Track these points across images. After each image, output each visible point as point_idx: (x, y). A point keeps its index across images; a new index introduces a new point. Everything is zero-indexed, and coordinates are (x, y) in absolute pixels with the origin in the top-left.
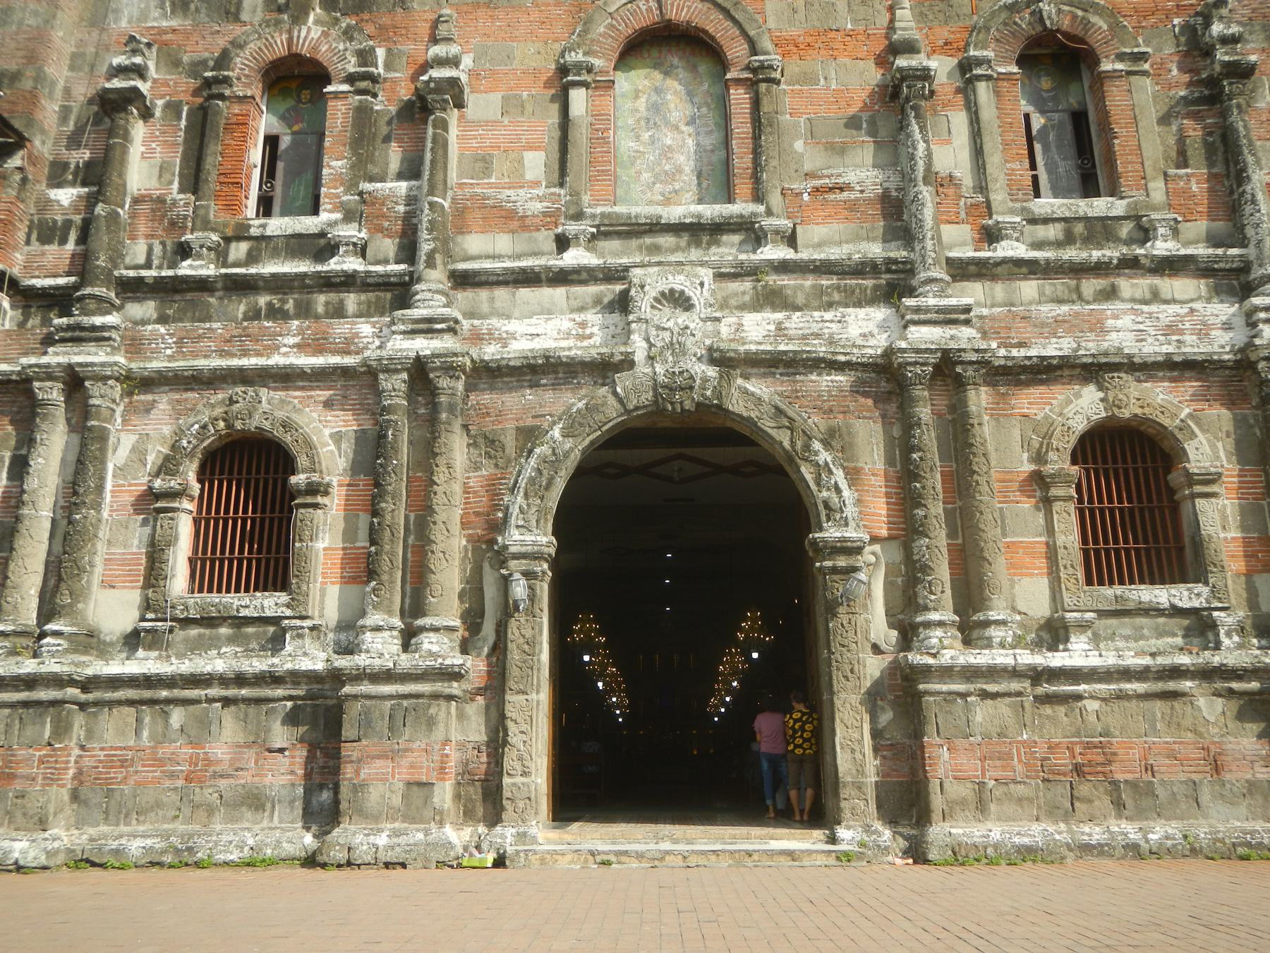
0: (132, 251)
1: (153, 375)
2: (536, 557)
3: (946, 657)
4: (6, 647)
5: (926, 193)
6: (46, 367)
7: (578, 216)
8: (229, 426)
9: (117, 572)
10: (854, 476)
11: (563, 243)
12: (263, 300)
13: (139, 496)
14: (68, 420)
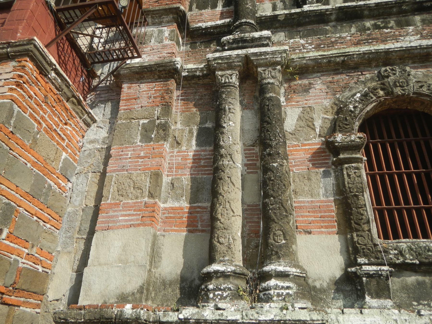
0: (261, 8)
1: (310, 62)
4: (229, 289)
6: (227, 59)
8: (387, 94)
9: (310, 219)
12: (368, 24)
13: (314, 153)
14: (241, 103)
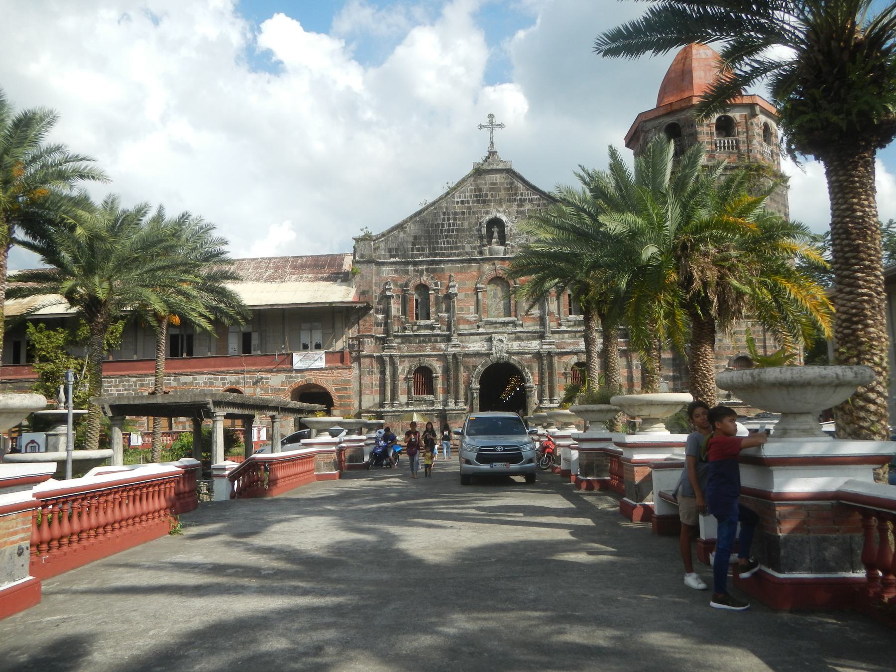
2: (477, 389)
3: (546, 406)
5: (547, 318)
7: (481, 321)
10: (532, 374)
11: (478, 327)
12: (422, 338)
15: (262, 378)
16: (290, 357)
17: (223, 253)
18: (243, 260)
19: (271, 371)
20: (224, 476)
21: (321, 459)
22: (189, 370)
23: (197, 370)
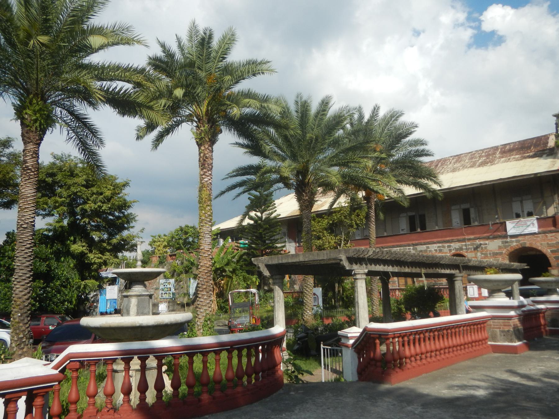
15: (481, 244)
16: (504, 225)
17: (411, 133)
18: (461, 155)
19: (488, 238)
20: (347, 346)
21: (496, 327)
22: (422, 241)
23: (429, 241)
